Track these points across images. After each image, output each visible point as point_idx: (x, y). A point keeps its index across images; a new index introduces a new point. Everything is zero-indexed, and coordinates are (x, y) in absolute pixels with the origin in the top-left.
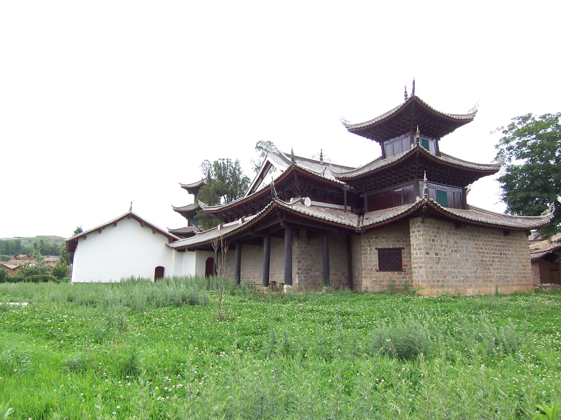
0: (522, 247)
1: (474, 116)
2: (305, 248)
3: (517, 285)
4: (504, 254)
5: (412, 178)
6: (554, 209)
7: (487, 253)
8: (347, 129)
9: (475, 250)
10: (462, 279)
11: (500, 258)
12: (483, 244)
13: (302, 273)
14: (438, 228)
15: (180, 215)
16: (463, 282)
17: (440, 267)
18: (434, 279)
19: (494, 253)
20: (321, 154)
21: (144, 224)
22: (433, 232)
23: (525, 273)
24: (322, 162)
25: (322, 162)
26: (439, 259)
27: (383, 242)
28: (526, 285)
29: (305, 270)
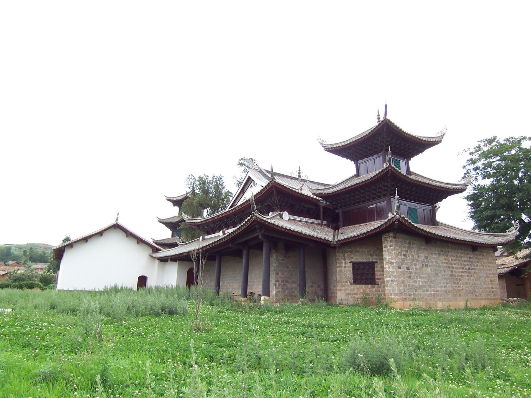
0: (489, 263)
1: (443, 138)
2: (282, 260)
3: (485, 299)
4: (472, 269)
5: (385, 195)
6: (519, 226)
7: (456, 268)
8: (323, 148)
9: (445, 265)
12: (452, 260)
13: (279, 285)
14: (410, 244)
15: (164, 226)
16: (434, 296)
18: (407, 292)
19: (463, 268)
20: (300, 171)
21: (129, 234)
22: (404, 247)
23: (492, 288)
24: (300, 179)
25: (300, 179)
26: (411, 273)
27: (356, 255)
28: (494, 299)
29: (282, 281)
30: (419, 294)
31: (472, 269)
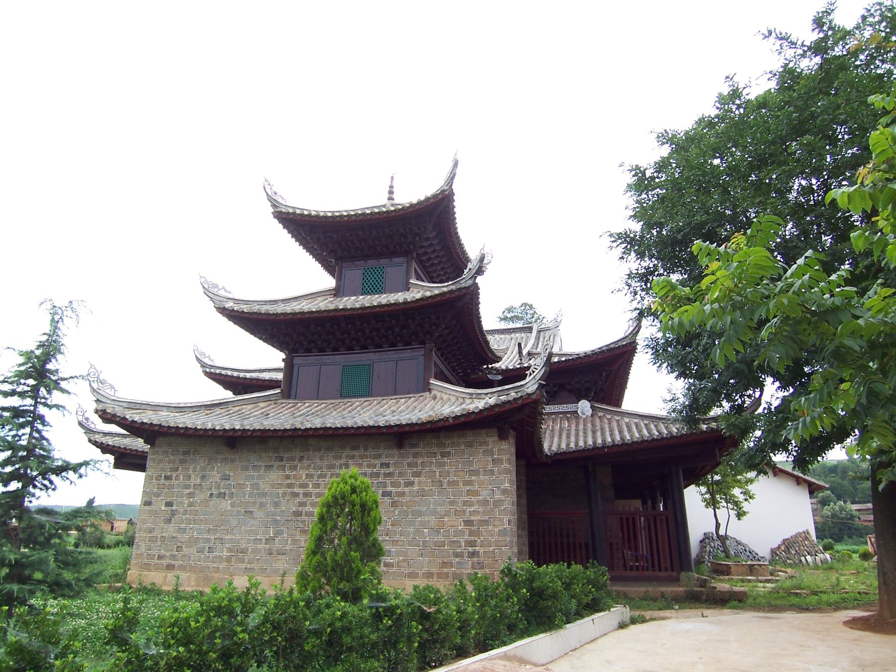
0: (475, 473)
9: (281, 491)
10: (226, 553)
12: (310, 476)
14: (185, 453)
18: (155, 552)
26: (173, 513)
30: (185, 556)
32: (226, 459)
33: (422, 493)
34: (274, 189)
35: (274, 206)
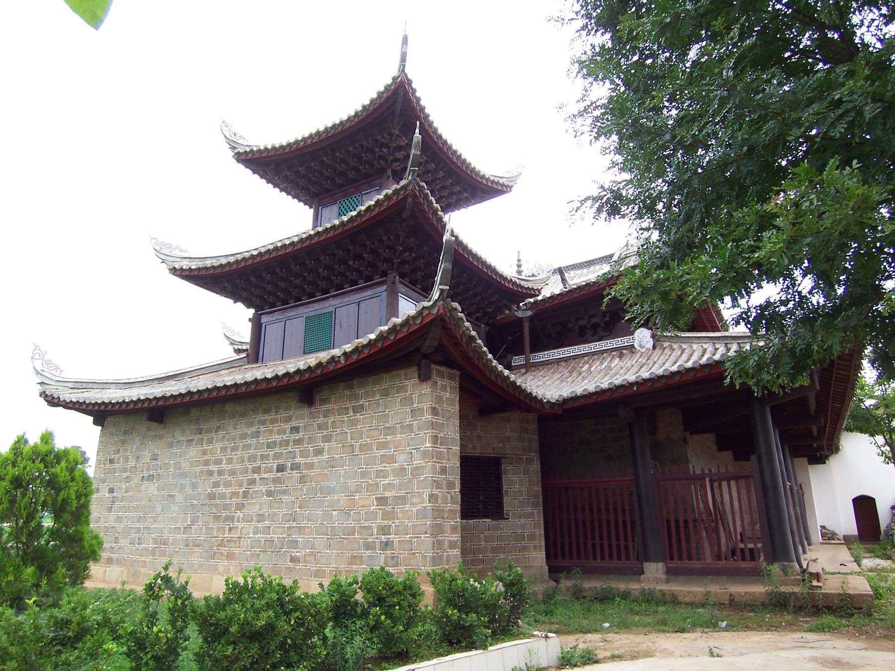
0: (390, 431)
4: (296, 467)
7: (233, 473)
9: (198, 469)
11: (276, 481)
12: (224, 449)
14: (126, 433)
16: (153, 554)
17: (112, 519)
19: (257, 470)
20: (519, 260)
31: (296, 467)
32: (156, 436)
33: (332, 464)
34: (234, 130)
35: (233, 148)
